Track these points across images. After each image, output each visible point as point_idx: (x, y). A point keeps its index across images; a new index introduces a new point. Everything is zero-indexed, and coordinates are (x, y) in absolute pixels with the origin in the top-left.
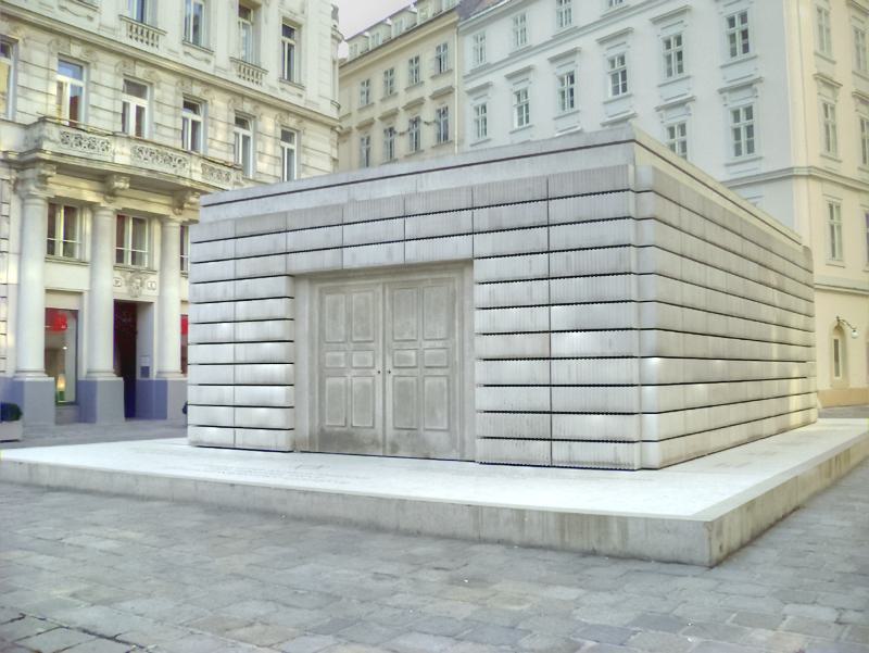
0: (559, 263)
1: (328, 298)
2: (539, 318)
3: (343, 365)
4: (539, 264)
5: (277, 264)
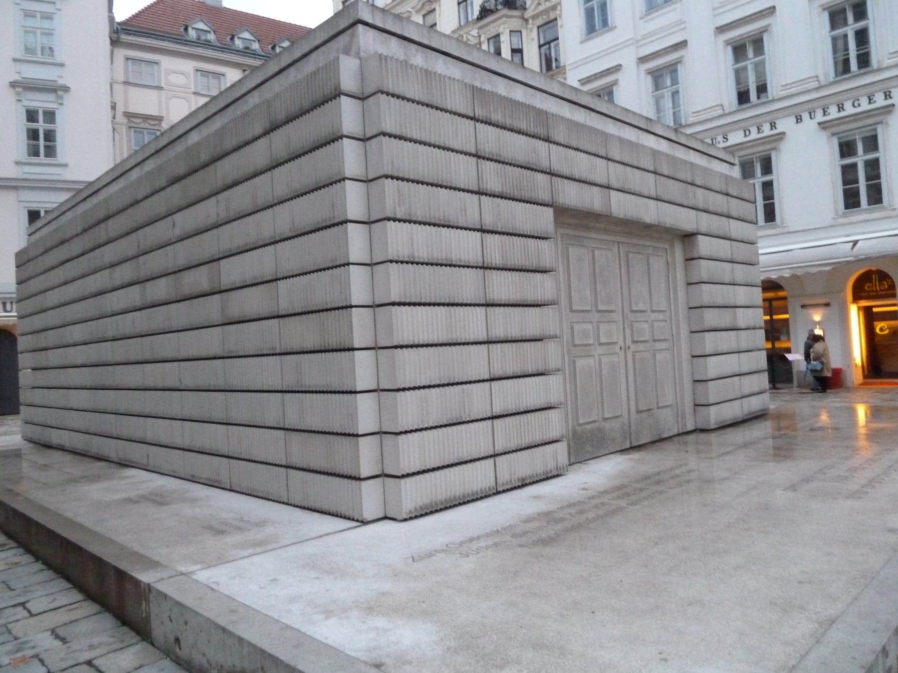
1: (573, 252)
3: (591, 342)
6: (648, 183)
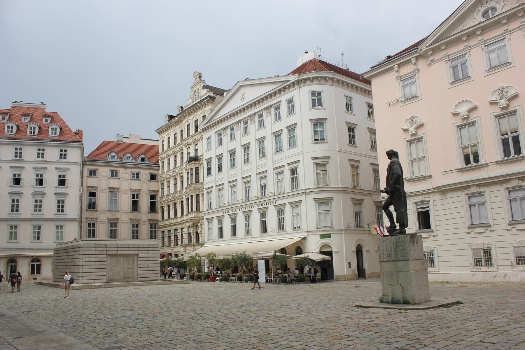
0: (150, 255)
2: (148, 262)
4: (147, 255)
5: (105, 252)
6: (127, 249)
